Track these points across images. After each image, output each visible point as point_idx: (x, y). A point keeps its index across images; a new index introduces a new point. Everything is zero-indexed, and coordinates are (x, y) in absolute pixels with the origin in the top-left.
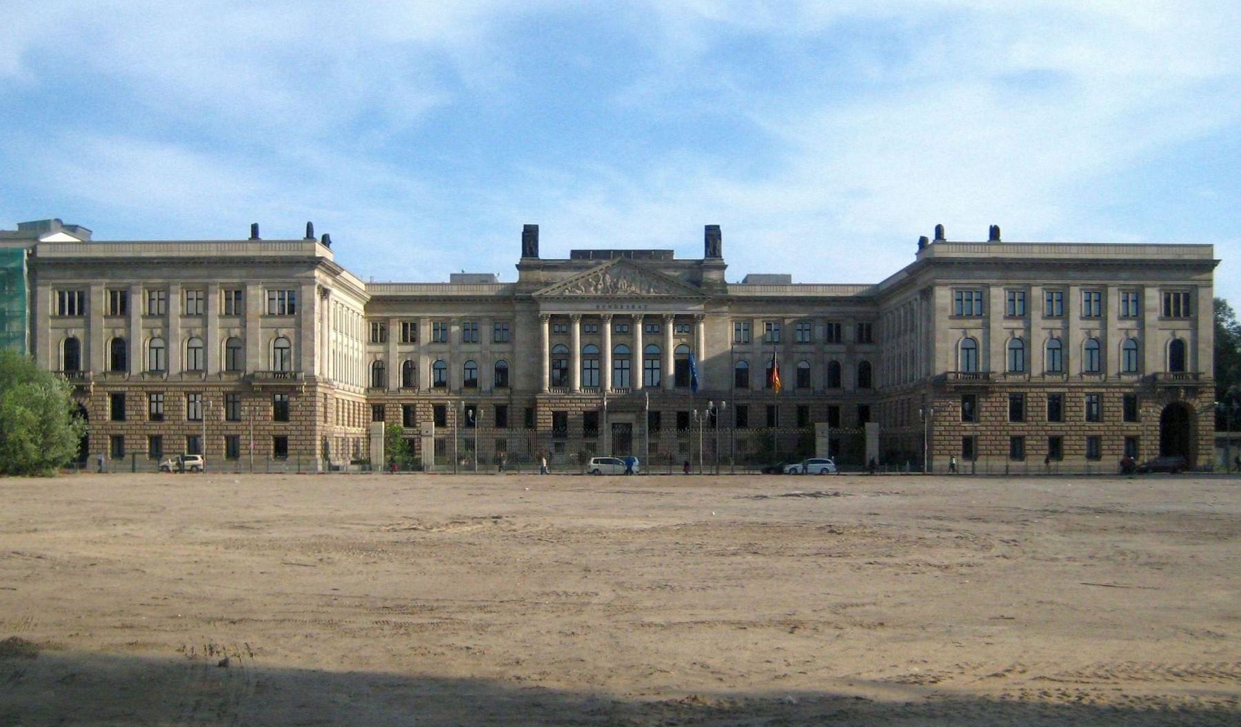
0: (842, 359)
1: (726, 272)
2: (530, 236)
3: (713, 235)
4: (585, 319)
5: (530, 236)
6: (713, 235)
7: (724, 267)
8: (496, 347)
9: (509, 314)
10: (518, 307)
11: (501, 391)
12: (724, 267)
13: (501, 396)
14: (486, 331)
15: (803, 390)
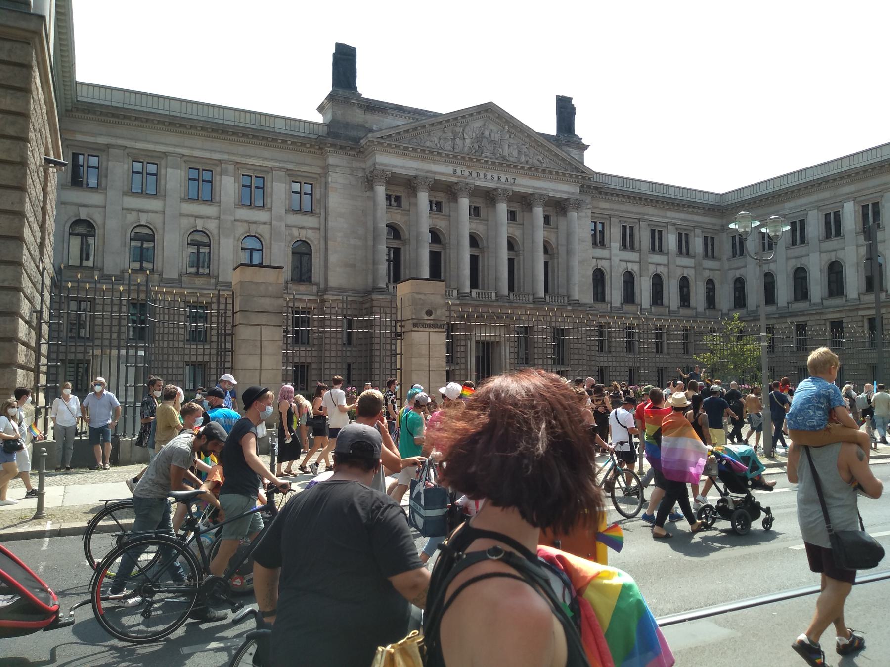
0: (690, 273)
1: (586, 153)
2: (344, 61)
3: (565, 110)
4: (436, 186)
5: (344, 61)
6: (565, 110)
7: (586, 147)
8: (294, 219)
9: (319, 171)
10: (332, 160)
11: (303, 288)
12: (586, 147)
13: (304, 294)
14: (279, 191)
15: (659, 309)
